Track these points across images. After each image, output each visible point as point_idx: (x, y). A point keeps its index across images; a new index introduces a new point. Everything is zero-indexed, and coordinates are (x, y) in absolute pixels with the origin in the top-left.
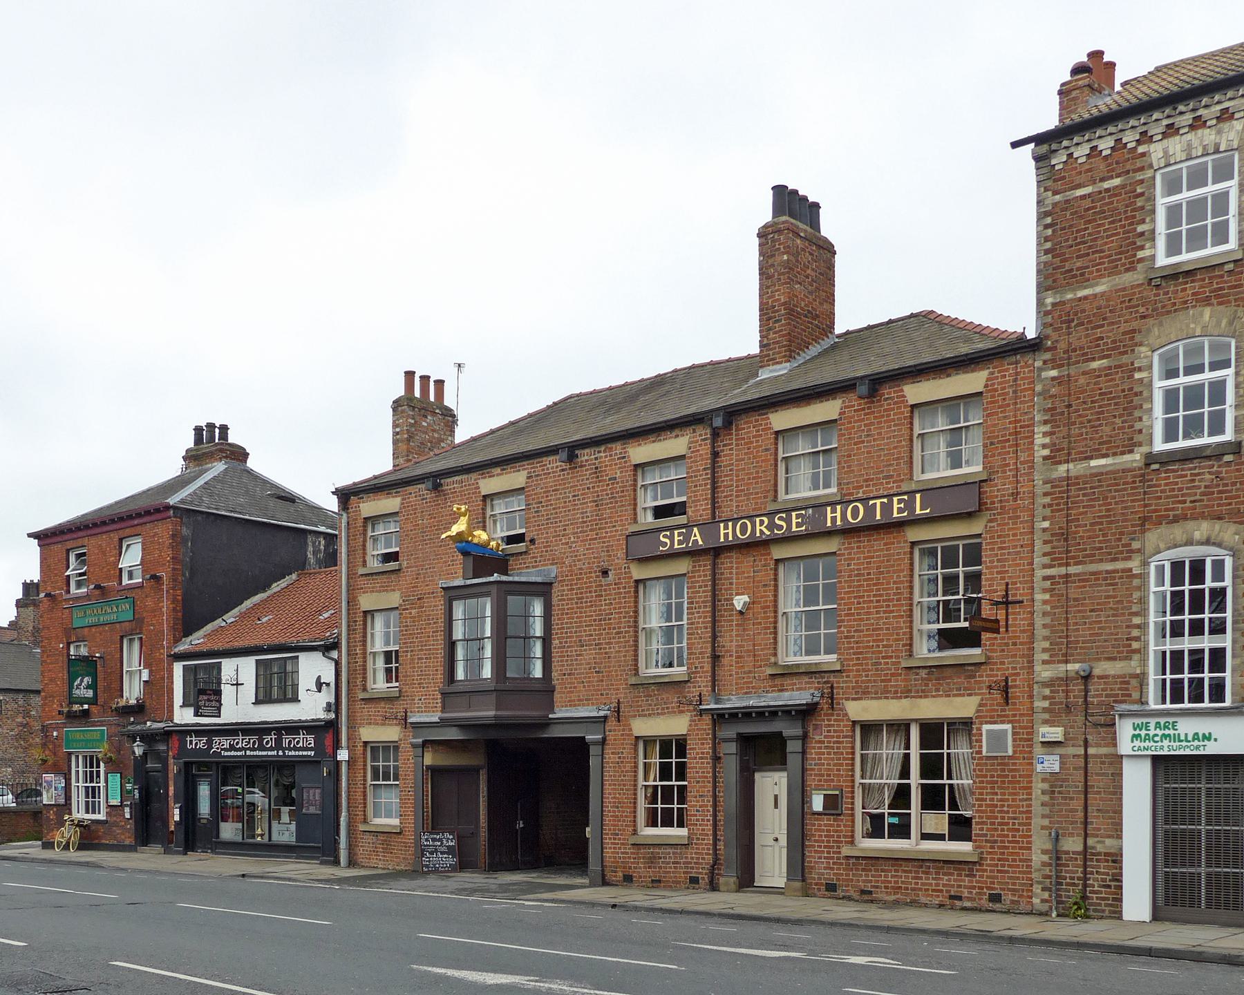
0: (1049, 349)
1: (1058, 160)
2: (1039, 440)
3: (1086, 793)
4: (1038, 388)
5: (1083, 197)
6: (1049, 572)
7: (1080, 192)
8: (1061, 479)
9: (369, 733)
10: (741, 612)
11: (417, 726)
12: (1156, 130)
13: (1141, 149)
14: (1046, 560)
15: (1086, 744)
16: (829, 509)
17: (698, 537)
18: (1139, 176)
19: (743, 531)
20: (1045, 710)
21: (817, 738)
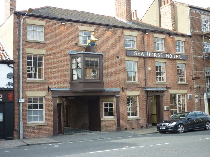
0: (192, 38)
1: (192, 11)
2: (192, 51)
3: (201, 105)
4: (191, 43)
5: (194, 18)
6: (194, 71)
7: (194, 17)
8: (195, 57)
9: (30, 94)
10: (150, 71)
11: (53, 92)
12: (202, 13)
13: (200, 15)
14: (194, 69)
15: (200, 98)
16: (167, 54)
17: (143, 54)
18: (200, 18)
19: (152, 55)
20: (195, 92)
21: (164, 96)
